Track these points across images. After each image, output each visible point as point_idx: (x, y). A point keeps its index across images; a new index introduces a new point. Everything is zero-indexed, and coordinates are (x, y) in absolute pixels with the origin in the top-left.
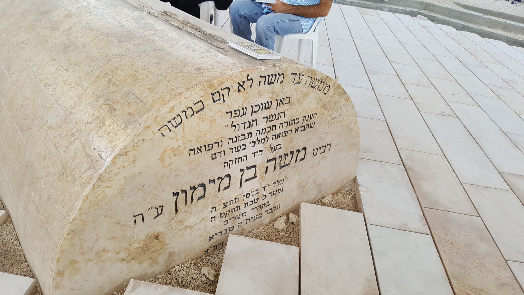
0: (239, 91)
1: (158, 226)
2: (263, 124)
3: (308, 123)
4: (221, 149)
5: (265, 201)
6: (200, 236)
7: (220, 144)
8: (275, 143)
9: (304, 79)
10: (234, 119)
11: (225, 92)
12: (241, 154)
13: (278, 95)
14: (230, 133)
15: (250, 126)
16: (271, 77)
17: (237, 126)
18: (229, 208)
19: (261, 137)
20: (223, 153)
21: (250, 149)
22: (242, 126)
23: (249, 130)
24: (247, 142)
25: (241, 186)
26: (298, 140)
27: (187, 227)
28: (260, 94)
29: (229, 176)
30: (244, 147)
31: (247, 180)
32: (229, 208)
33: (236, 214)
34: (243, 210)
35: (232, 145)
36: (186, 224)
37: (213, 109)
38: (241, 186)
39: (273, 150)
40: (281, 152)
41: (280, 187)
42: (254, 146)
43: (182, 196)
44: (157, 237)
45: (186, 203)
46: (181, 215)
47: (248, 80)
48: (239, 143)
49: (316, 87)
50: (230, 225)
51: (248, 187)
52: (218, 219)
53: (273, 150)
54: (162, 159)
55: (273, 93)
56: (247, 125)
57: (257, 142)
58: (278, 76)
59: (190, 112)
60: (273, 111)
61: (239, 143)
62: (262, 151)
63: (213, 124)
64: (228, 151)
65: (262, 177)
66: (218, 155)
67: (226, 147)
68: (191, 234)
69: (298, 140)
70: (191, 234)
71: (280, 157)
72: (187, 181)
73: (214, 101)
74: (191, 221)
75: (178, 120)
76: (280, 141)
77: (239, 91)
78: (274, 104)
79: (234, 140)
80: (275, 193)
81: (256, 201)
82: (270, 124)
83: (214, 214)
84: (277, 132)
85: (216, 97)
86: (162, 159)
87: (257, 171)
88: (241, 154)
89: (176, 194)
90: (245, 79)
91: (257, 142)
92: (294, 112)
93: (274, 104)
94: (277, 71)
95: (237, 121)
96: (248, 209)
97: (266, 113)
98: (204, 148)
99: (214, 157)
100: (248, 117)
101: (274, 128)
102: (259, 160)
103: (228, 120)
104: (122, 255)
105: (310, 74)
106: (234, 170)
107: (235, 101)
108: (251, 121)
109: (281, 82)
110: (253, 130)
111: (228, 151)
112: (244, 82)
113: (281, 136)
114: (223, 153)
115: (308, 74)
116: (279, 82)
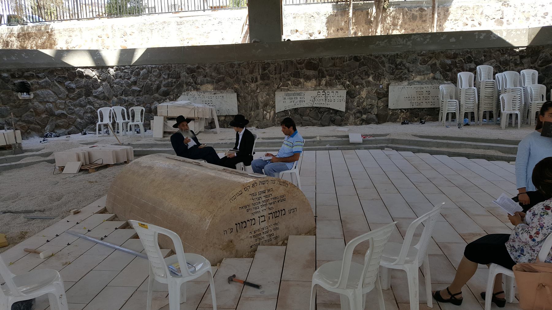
1: (232, 237)
2: (264, 199)
3: (282, 199)
5: (271, 233)
8: (270, 206)
9: (276, 182)
12: (258, 210)
14: (252, 202)
18: (256, 234)
19: (264, 204)
21: (261, 209)
24: (259, 205)
26: (281, 206)
28: (260, 188)
29: (254, 219)
32: (256, 234)
33: (260, 237)
34: (262, 236)
36: (241, 238)
37: (245, 193)
40: (274, 210)
44: (231, 242)
46: (239, 234)
48: (256, 206)
50: (258, 242)
51: (264, 225)
54: (231, 210)
60: (267, 194)
61: (256, 206)
63: (245, 199)
65: (268, 221)
67: (251, 207)
69: (281, 206)
72: (240, 220)
74: (243, 237)
76: (272, 205)
78: (267, 191)
82: (267, 199)
83: (251, 235)
86: (231, 210)
88: (258, 210)
89: (236, 224)
92: (275, 194)
93: (267, 191)
95: (254, 197)
96: (265, 235)
97: (264, 195)
100: (258, 196)
102: (265, 213)
103: (251, 197)
104: (221, 247)
106: (256, 216)
107: (252, 190)
110: (261, 201)
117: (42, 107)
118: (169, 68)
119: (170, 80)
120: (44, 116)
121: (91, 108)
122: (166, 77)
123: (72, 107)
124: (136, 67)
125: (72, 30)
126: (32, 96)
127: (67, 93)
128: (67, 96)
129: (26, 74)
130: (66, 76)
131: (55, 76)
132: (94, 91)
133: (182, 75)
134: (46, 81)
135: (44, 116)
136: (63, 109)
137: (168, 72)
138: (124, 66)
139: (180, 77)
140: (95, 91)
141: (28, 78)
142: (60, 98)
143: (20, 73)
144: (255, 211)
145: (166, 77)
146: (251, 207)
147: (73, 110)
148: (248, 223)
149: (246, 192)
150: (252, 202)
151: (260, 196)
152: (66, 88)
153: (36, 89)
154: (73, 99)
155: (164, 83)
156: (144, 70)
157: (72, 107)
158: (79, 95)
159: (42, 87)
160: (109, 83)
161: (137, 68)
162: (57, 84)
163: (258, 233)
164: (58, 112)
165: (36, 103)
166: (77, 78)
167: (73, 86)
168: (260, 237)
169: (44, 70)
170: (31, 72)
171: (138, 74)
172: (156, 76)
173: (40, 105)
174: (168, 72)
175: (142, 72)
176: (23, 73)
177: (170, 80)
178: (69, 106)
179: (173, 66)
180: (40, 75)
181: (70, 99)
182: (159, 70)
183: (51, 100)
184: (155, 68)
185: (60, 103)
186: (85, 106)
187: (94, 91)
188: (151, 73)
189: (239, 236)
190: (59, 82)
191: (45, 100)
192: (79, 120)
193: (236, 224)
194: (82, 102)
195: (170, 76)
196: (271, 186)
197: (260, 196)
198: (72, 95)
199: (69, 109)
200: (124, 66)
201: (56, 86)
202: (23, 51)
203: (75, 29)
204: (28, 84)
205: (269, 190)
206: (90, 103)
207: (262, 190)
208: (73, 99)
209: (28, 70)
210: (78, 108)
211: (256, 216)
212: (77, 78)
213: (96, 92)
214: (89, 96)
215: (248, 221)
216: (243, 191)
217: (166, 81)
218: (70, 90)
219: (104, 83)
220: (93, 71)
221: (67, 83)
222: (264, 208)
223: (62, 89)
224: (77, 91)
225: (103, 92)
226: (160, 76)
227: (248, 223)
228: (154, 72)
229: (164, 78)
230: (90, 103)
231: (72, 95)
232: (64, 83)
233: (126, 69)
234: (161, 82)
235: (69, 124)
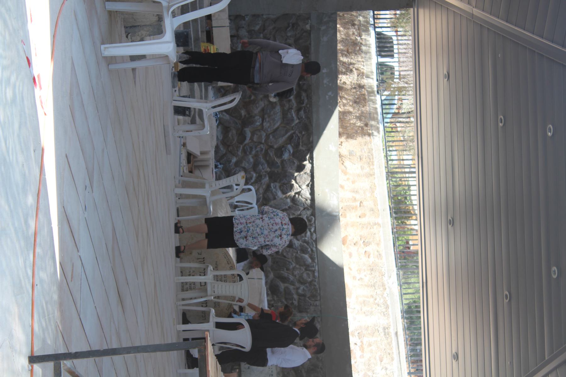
117: (256, 111)
118: (313, 296)
119: (295, 297)
120: (243, 112)
121: (251, 178)
122: (300, 291)
123: (254, 152)
124: (314, 249)
125: (370, 162)
126: (273, 100)
127: (275, 147)
128: (271, 147)
129: (304, 94)
130: (301, 148)
131: (301, 132)
132: (278, 185)
133: (304, 314)
134: (293, 120)
135: (243, 112)
136: (251, 139)
137: (308, 295)
138: (315, 231)
139: (300, 312)
140: (278, 187)
141: (298, 96)
142: (268, 136)
143: (305, 87)
145: (300, 291)
147: (250, 153)
152: (283, 146)
153: (282, 106)
154: (266, 154)
155: (291, 287)
156: (310, 260)
157: (254, 152)
158: (271, 164)
159: (285, 114)
160: (289, 207)
161: (312, 250)
162: (289, 134)
164: (248, 132)
165: (262, 104)
166: (296, 163)
167: (286, 156)
169: (309, 118)
170: (306, 101)
171: (304, 251)
172: (301, 277)
173: (259, 109)
174: (308, 295)
175: (307, 256)
176: (306, 91)
177: (295, 297)
178: (256, 148)
179: (318, 303)
180: (302, 112)
181: (266, 151)
182: (311, 282)
183: (266, 125)
184: (314, 276)
185: (261, 136)
186: (255, 170)
187: (278, 185)
188: (306, 270)
190: (291, 138)
191: (266, 116)
192: (234, 160)
194: (260, 167)
195: (302, 298)
198: (272, 153)
199: (251, 148)
200: (315, 231)
201: (286, 133)
202: (335, 90)
203: (371, 167)
204: (290, 96)
206: (259, 178)
208: (266, 154)
209: (309, 97)
210: (252, 160)
212: (296, 163)
213: (275, 188)
214: (270, 177)
217: (293, 292)
218: (280, 151)
219: (289, 200)
220: (308, 185)
221: (290, 147)
223: (281, 141)
224: (278, 161)
225: (275, 199)
226: (302, 282)
228: (308, 274)
229: (298, 289)
230: (259, 178)
231: (272, 153)
232: (290, 144)
233: (311, 234)
234: (292, 283)
235: (229, 146)
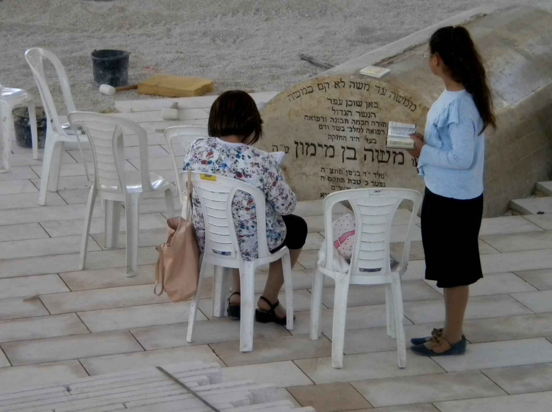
0: (336, 87)
2: (357, 117)
4: (327, 124)
6: (314, 188)
7: (325, 120)
8: (370, 136)
9: (388, 93)
10: (334, 106)
11: (326, 85)
12: (341, 134)
13: (366, 99)
14: (330, 114)
15: (346, 114)
16: (358, 85)
17: (336, 112)
19: (356, 126)
20: (327, 127)
22: (340, 112)
23: (345, 117)
24: (346, 125)
25: (343, 161)
27: (304, 173)
28: (352, 95)
30: (342, 129)
31: (348, 158)
35: (334, 124)
37: (318, 94)
38: (343, 161)
39: (369, 141)
40: (377, 147)
41: (382, 181)
42: (351, 131)
43: (300, 146)
45: (303, 153)
47: (341, 82)
49: (402, 102)
51: (350, 165)
52: (326, 182)
53: (369, 141)
55: (362, 95)
56: (344, 113)
57: (353, 130)
58: (364, 85)
59: (304, 91)
60: (364, 109)
62: (358, 138)
64: (331, 127)
65: (361, 162)
66: (324, 128)
68: (306, 181)
70: (306, 181)
71: (377, 151)
72: (305, 138)
73: (320, 89)
74: (307, 169)
75: (298, 94)
77: (336, 87)
78: (364, 105)
79: (335, 120)
80: (377, 184)
81: (359, 182)
83: (323, 174)
84: (371, 128)
85: (321, 87)
87: (357, 155)
88: (341, 134)
89: (296, 143)
90: (339, 81)
91: (353, 130)
93: (364, 105)
94: (363, 81)
95: (336, 107)
97: (358, 109)
98: (313, 118)
99: (321, 127)
100: (344, 107)
101: (367, 123)
102: (357, 145)
105: (393, 90)
107: (334, 93)
108: (346, 110)
109: (368, 90)
110: (349, 118)
111: (331, 127)
112: (338, 82)
113: (374, 131)
114: (327, 127)
115: (391, 90)
116: (366, 89)
144: (335, 132)
146: (329, 123)
148: (319, 149)
149: (321, 93)
150: (330, 114)
151: (349, 108)
163: (337, 175)
168: (342, 185)
189: (300, 166)
193: (296, 143)
196: (374, 97)
197: (349, 108)
205: (369, 105)
207: (356, 98)
211: (338, 144)
215: (320, 145)
216: (316, 88)
222: (356, 134)
227: (319, 149)
